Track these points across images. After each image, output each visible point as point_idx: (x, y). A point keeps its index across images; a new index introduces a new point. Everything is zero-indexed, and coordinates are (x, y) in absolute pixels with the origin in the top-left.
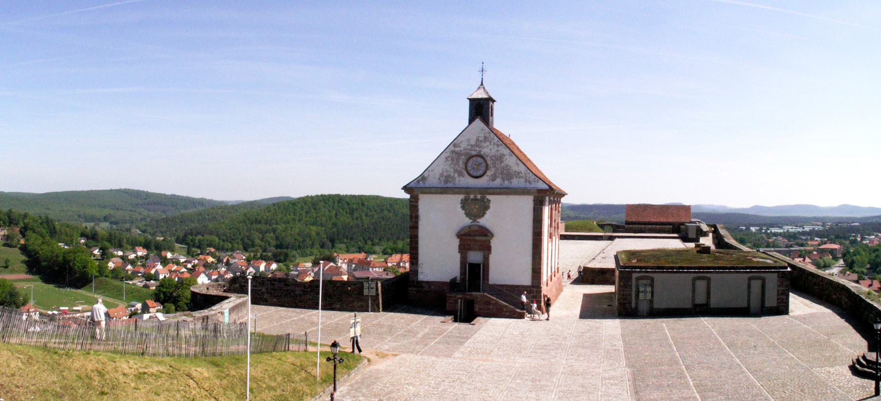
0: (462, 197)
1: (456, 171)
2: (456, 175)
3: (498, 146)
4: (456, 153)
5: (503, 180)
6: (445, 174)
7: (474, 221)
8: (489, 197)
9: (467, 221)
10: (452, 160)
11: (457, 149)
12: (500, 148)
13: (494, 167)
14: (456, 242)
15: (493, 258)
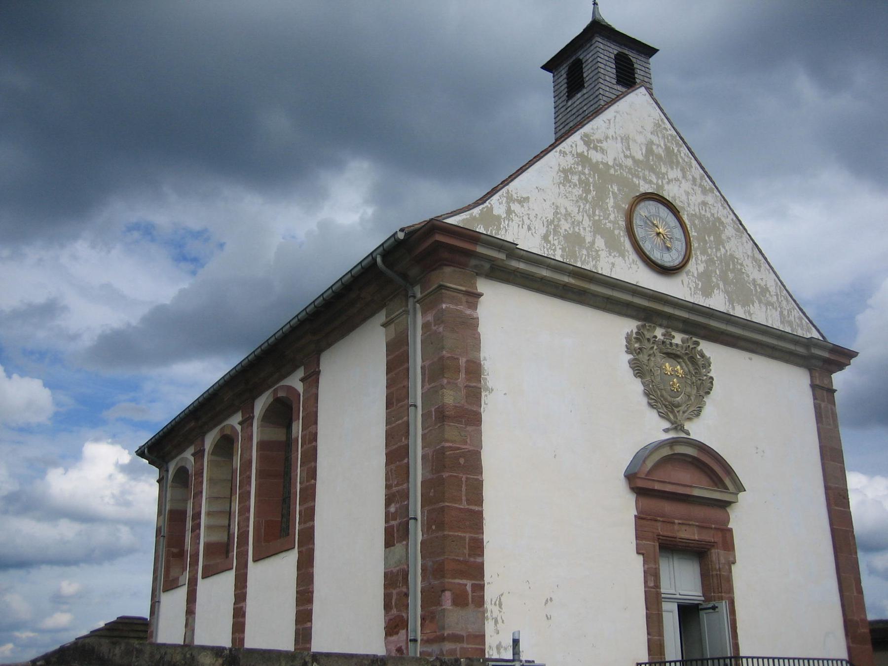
0: (630, 326)
1: (597, 228)
2: (600, 243)
3: (705, 191)
4: (594, 167)
5: (731, 302)
6: (565, 226)
7: (678, 427)
8: (707, 348)
9: (654, 429)
10: (584, 184)
11: (595, 156)
12: (710, 199)
13: (704, 252)
14: (627, 506)
15: (743, 577)
